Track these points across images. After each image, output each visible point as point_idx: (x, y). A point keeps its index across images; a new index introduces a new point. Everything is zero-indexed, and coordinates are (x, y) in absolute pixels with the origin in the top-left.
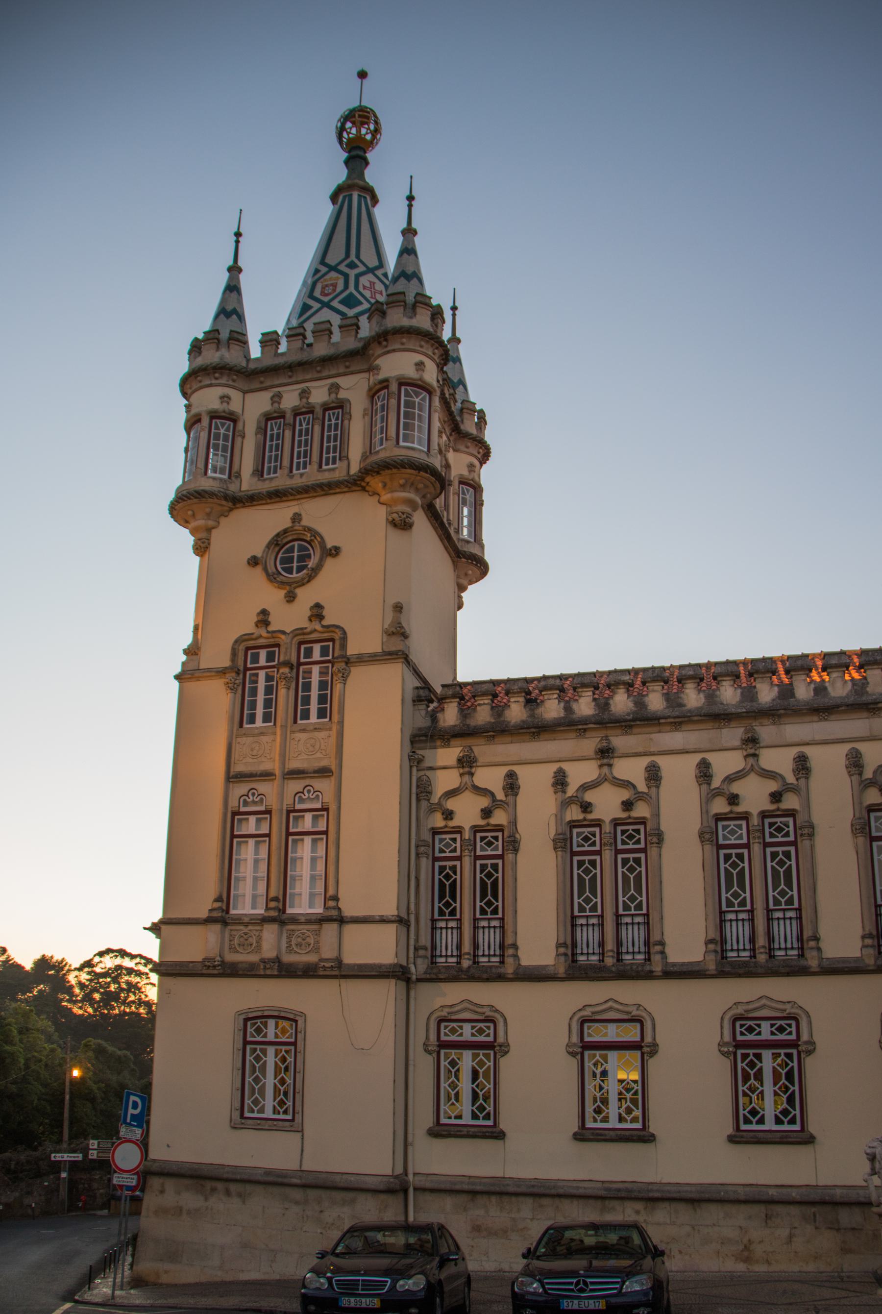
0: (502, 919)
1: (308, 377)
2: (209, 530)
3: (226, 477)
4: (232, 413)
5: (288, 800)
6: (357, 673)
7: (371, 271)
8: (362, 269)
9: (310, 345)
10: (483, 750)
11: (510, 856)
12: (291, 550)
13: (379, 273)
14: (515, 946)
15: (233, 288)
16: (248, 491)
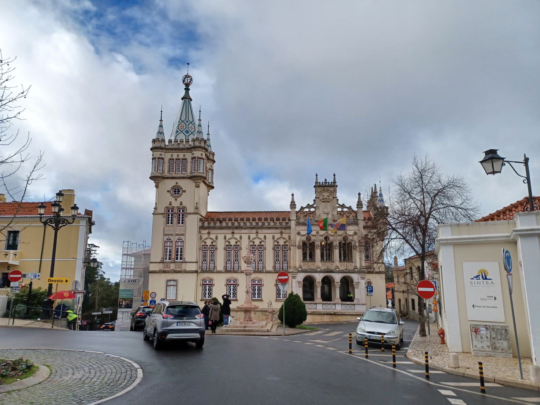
0: (214, 262)
1: (179, 152)
2: (158, 183)
3: (162, 172)
4: (163, 158)
5: (176, 240)
6: (189, 216)
7: (191, 123)
8: (189, 122)
9: (179, 144)
10: (212, 231)
11: (216, 251)
12: (176, 189)
13: (193, 123)
14: (216, 267)
15: (161, 126)
16: (166, 176)
